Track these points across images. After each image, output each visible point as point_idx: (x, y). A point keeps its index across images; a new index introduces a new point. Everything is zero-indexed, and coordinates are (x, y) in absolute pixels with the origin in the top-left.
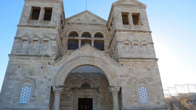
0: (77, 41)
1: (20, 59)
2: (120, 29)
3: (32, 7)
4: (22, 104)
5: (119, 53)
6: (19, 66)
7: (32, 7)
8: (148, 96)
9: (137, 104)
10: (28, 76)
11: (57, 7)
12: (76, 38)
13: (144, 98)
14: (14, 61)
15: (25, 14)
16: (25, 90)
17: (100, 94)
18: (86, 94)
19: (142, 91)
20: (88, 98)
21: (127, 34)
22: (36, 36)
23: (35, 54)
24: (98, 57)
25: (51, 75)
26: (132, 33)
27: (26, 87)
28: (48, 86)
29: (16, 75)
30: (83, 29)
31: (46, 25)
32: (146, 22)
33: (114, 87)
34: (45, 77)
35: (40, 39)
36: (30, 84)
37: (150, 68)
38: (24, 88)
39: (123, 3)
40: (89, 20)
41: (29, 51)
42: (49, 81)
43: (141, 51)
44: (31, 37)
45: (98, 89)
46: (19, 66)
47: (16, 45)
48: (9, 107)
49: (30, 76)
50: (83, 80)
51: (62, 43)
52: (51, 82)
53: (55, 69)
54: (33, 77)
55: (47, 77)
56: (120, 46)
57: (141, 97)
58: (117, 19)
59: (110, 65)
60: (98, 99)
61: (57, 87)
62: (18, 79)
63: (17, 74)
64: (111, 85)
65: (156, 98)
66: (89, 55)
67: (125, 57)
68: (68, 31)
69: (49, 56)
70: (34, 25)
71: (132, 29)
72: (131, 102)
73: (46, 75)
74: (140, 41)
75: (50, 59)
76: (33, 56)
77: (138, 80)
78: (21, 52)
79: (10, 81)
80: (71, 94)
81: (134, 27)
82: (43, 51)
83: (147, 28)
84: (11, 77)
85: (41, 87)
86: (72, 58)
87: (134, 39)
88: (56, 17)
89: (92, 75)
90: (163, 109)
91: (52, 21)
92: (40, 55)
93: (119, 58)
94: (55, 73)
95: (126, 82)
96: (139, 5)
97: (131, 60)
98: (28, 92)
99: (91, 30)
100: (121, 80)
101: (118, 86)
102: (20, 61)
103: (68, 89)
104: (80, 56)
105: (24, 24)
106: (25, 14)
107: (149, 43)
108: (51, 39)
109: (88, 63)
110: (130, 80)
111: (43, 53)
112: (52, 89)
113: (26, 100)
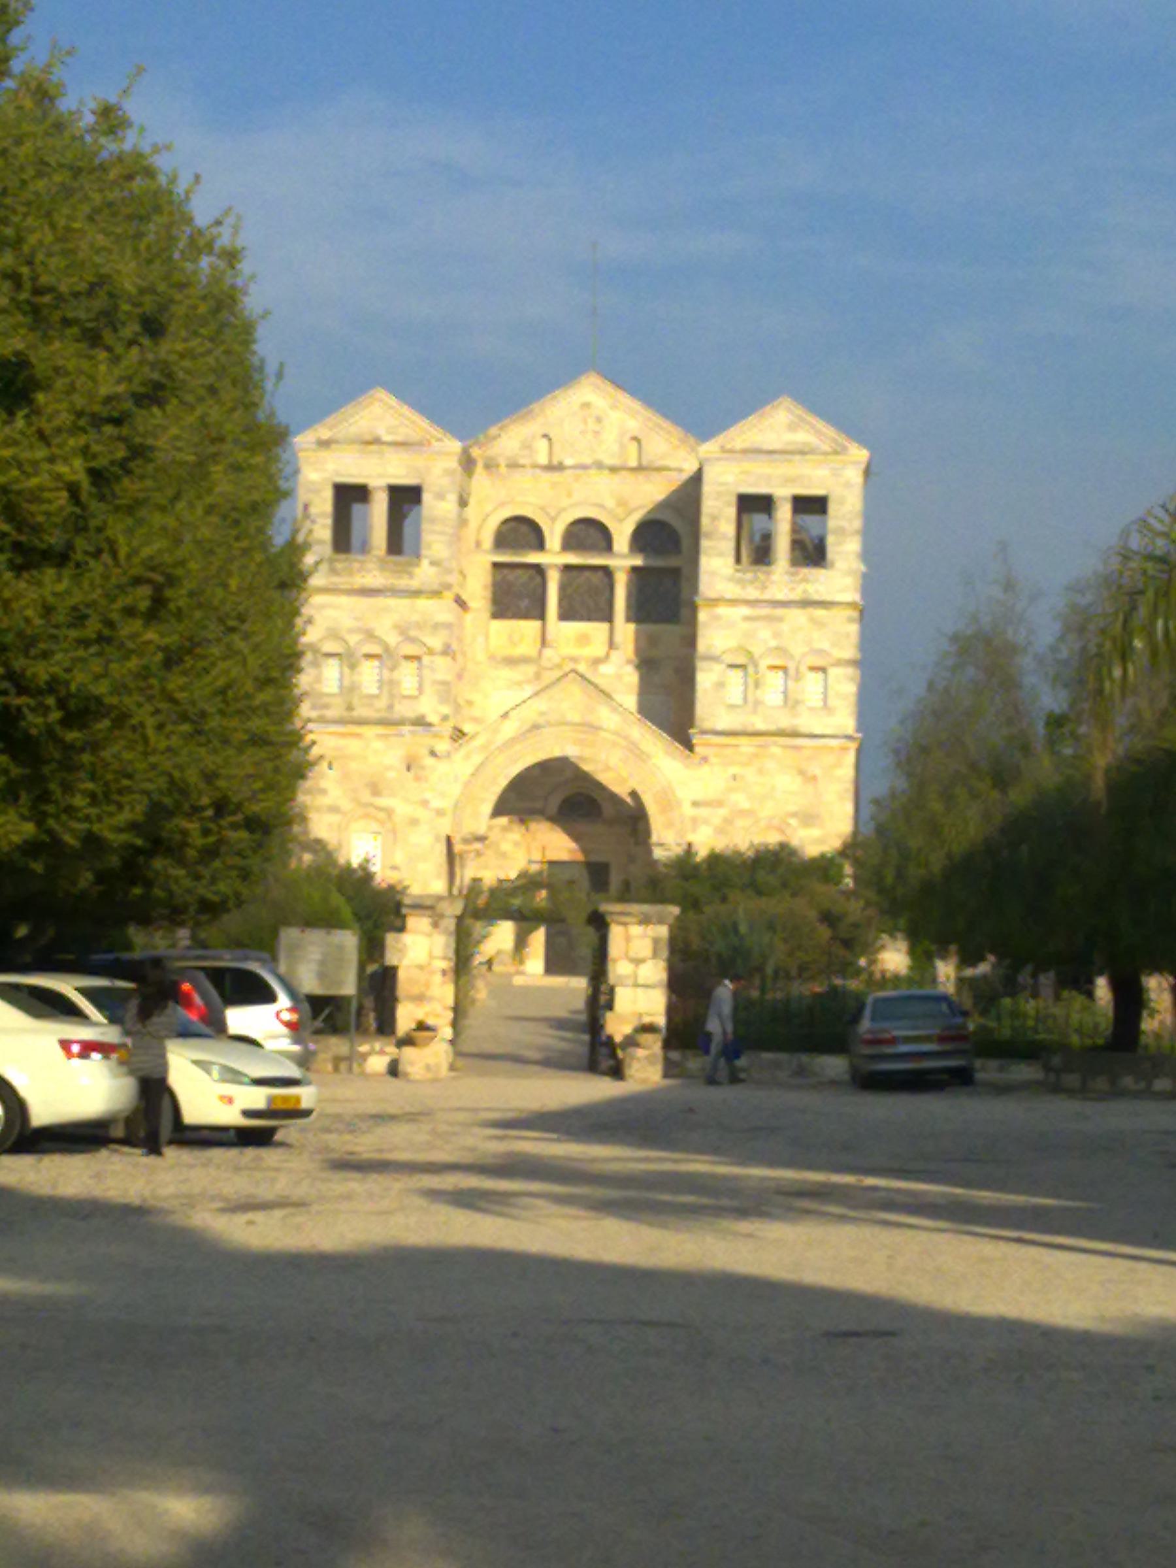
0: (539, 570)
12: (533, 558)
21: (747, 619)
22: (370, 635)
31: (403, 582)
34: (425, 803)
35: (387, 649)
36: (375, 826)
37: (818, 772)
41: (356, 701)
44: (353, 639)
54: (382, 802)
56: (706, 678)
61: (466, 841)
62: (334, 809)
64: (654, 838)
67: (721, 726)
68: (488, 516)
69: (430, 725)
73: (428, 795)
74: (797, 650)
78: (326, 706)
87: (773, 643)
91: (425, 563)
94: (455, 790)
97: (743, 740)
99: (610, 503)
101: (679, 841)
104: (541, 721)
107: (839, 663)
108: (431, 652)
110: (728, 821)
111: (404, 710)
112: (449, 841)
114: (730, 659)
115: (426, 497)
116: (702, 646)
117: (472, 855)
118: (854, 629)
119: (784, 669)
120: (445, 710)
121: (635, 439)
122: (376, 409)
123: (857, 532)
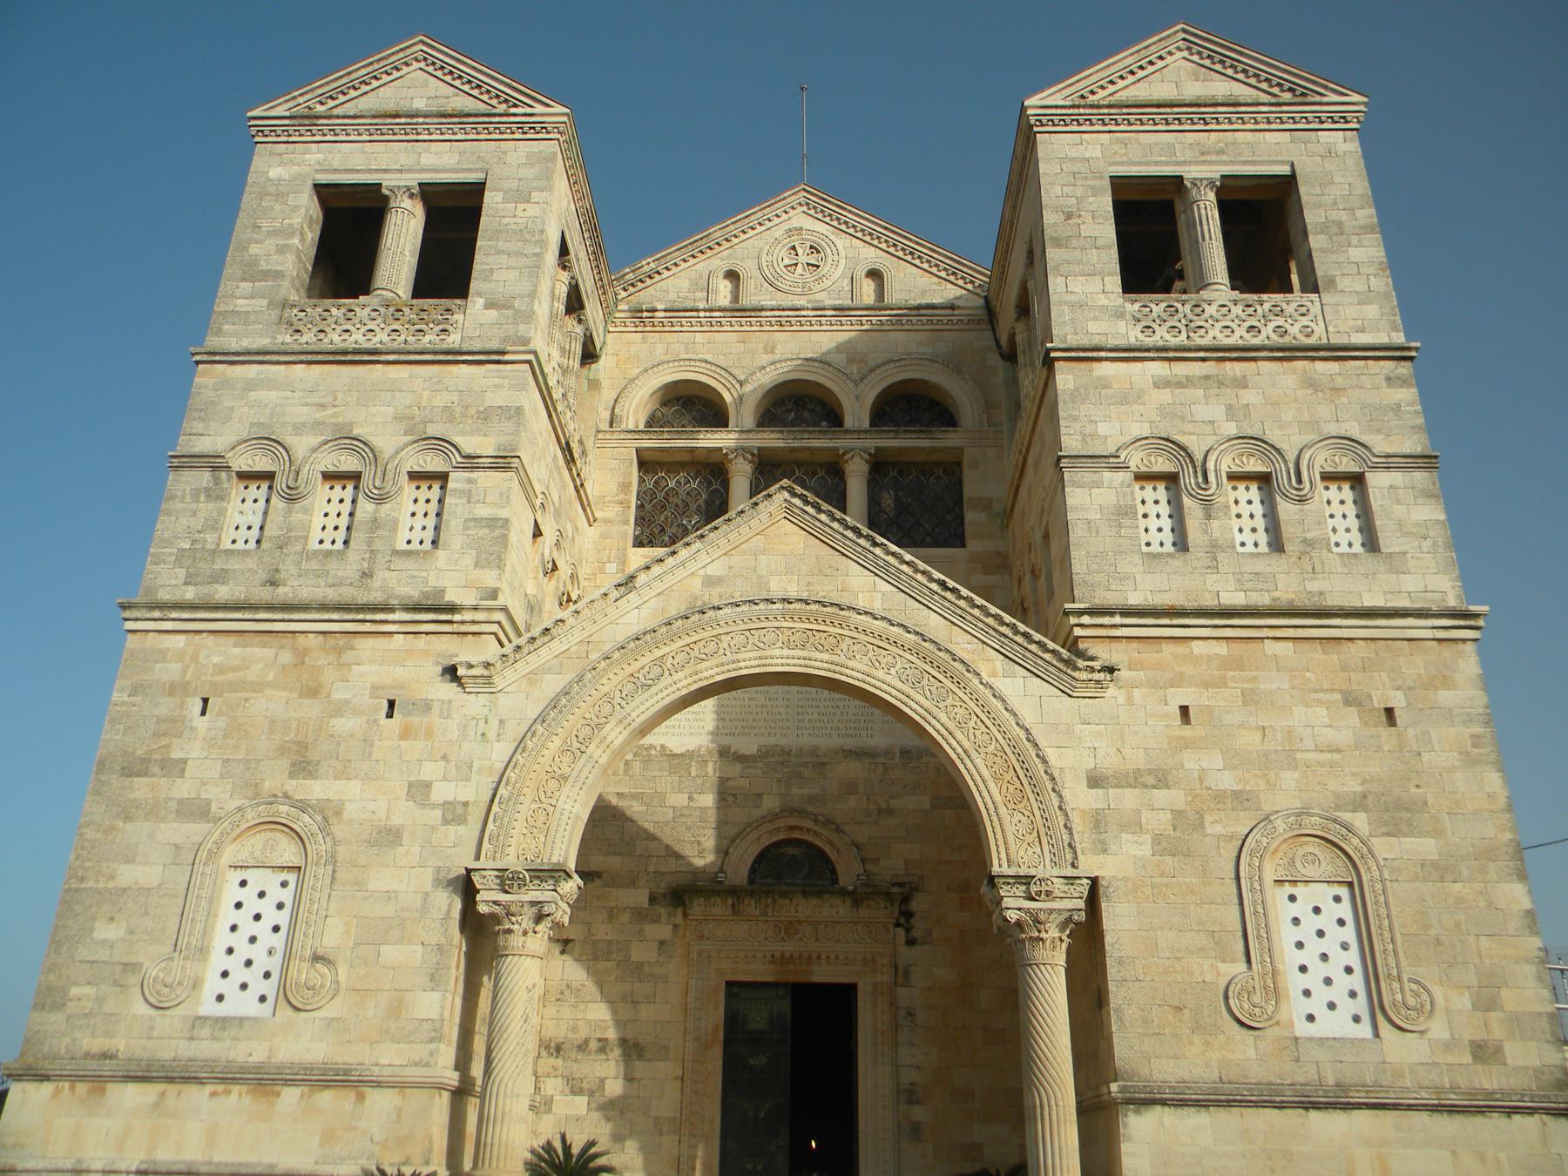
1: (210, 640)
2: (1096, 341)
3: (318, 187)
4: (224, 1022)
5: (1080, 564)
6: (205, 701)
7: (315, 185)
8: (1372, 976)
9: (1262, 1045)
10: (275, 778)
11: (523, 173)
13: (1338, 993)
14: (162, 655)
15: (255, 249)
16: (253, 905)
17: (918, 947)
18: (790, 947)
19: (1311, 923)
20: (815, 979)
21: (1161, 383)
23: (332, 595)
24: (877, 607)
25: (465, 770)
26: (1209, 368)
27: (257, 879)
28: (438, 869)
29: (183, 771)
30: (765, 359)
31: (429, 340)
32: (1356, 254)
33: (1027, 880)
34: (419, 791)
36: (288, 852)
38: (243, 883)
39: (1123, 96)
40: (824, 270)
41: (288, 568)
42: (452, 828)
43: (1305, 541)
44: (301, 445)
45: (906, 899)
46: (205, 701)
47: (184, 521)
48: (120, 1044)
49: (291, 786)
50: (776, 817)
51: (579, 488)
52: (461, 828)
53: (501, 722)
54: (315, 789)
55: (428, 785)
57: (1299, 982)
58: (1058, 243)
59: (994, 674)
60: (902, 992)
61: (507, 880)
62: (196, 810)
63: (189, 762)
65: (1463, 1002)
66: (793, 594)
67: (1135, 599)
69: (452, 609)
70: (335, 339)
71: (1215, 335)
72: (1197, 1027)
73: (430, 771)
75: (455, 628)
76: (324, 607)
77: (1267, 818)
78: (220, 577)
79: (129, 827)
80: (662, 943)
81: (1237, 310)
82: (399, 563)
83: (1372, 311)
84: (141, 788)
85: (378, 881)
86: (650, 625)
87: (1231, 429)
88: (513, 262)
89: (854, 769)
90: (1531, 1111)
91: (476, 303)
92: (376, 597)
93: (1080, 613)
94: (499, 752)
95: (1148, 838)
96: (1287, 96)
97: (1200, 628)
98: (271, 916)
100: (1097, 812)
101: (1070, 872)
102: (217, 653)
103: (640, 897)
105: (246, 343)
106: (255, 249)
108: (471, 462)
109: (782, 659)
110: (1188, 821)
111: (399, 582)
113: (258, 986)
114: (1137, 460)
115: (490, 199)
116: (1071, 442)
117: (526, 921)
118: (1407, 395)
119: (1264, 480)
120: (489, 578)
121: (874, 274)
122: (415, 75)
123: (1369, 229)
